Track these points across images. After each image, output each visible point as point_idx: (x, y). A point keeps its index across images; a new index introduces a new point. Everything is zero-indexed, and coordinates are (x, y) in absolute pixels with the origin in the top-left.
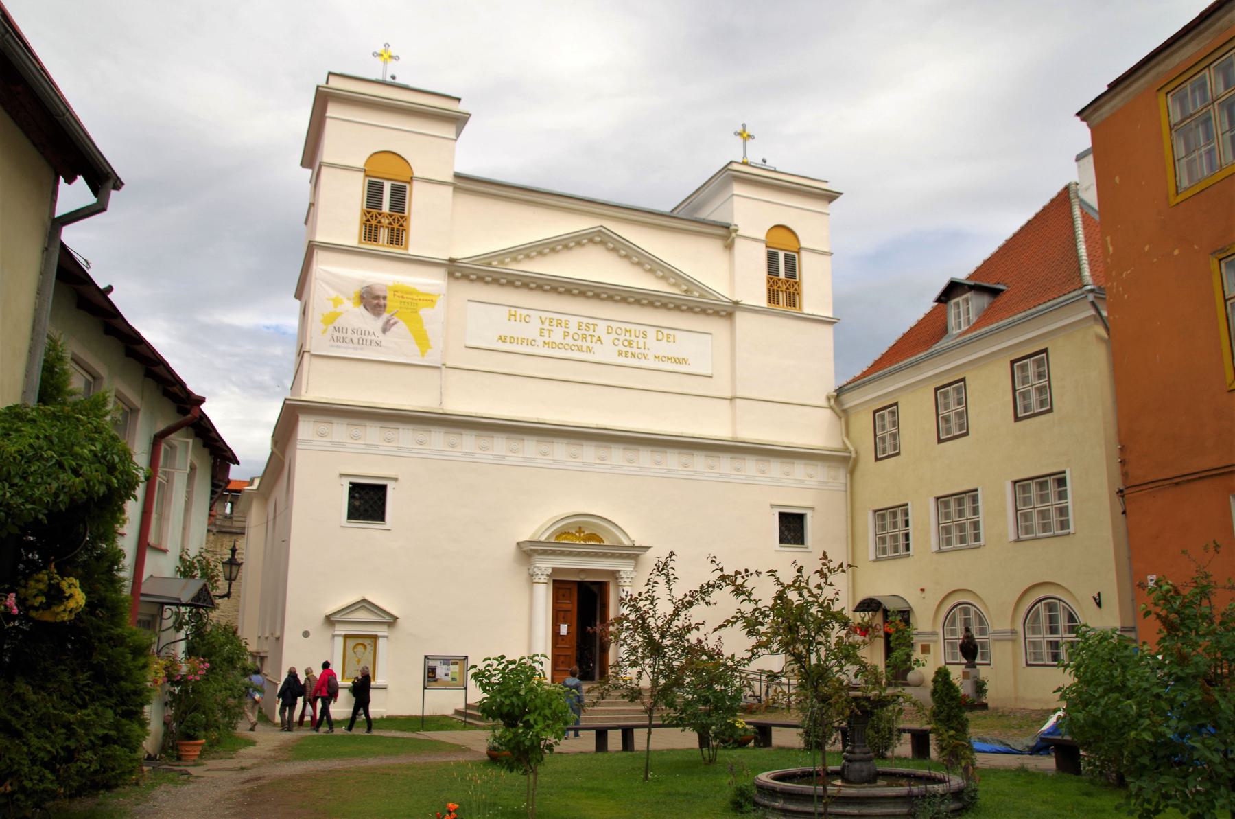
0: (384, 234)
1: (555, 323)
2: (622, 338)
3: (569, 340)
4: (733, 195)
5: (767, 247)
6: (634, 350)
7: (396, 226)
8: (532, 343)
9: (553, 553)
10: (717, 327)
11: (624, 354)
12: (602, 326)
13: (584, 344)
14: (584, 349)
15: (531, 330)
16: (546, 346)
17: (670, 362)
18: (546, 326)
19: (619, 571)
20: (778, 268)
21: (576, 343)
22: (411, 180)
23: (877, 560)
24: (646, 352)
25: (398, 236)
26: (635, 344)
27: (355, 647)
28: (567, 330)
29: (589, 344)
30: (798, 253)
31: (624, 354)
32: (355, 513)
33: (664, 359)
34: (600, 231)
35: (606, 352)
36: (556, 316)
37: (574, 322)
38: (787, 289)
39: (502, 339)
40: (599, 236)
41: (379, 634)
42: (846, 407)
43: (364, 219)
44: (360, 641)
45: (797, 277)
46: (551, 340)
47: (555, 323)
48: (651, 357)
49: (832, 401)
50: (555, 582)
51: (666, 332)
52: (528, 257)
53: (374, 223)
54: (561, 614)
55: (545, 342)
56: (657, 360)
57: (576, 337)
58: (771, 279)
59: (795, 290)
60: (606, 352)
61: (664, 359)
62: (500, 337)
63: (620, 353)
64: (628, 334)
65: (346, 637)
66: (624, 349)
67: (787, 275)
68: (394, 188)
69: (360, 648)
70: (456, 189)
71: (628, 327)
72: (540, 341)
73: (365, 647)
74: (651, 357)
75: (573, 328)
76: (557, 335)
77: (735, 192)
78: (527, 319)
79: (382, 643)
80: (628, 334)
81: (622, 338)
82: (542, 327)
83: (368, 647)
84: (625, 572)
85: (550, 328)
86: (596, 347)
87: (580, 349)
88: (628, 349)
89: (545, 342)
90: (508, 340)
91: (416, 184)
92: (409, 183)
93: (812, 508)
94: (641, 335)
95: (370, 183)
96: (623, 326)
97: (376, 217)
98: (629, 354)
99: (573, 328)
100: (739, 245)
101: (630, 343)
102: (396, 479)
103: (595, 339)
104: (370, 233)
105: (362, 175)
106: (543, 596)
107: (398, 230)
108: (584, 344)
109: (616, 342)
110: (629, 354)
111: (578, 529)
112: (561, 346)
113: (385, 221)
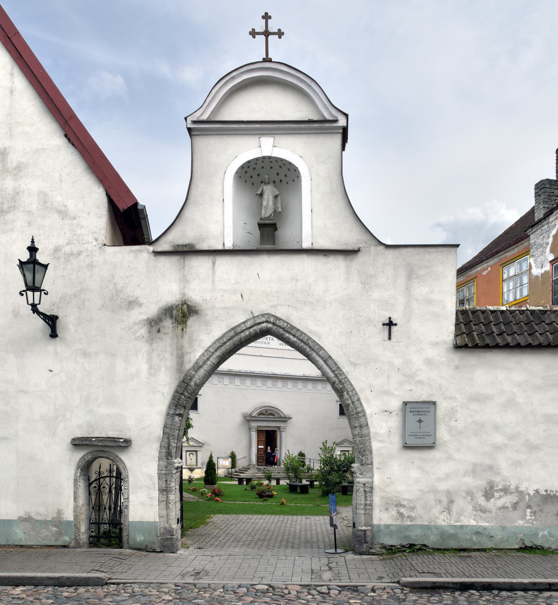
9: (258, 420)
14: (267, 343)
19: (280, 426)
27: (190, 454)
29: (268, 341)
44: (191, 452)
50: (258, 430)
54: (260, 442)
65: (187, 451)
69: (191, 455)
73: (193, 455)
79: (199, 453)
84: (283, 427)
87: (265, 343)
103: (271, 339)
106: (254, 435)
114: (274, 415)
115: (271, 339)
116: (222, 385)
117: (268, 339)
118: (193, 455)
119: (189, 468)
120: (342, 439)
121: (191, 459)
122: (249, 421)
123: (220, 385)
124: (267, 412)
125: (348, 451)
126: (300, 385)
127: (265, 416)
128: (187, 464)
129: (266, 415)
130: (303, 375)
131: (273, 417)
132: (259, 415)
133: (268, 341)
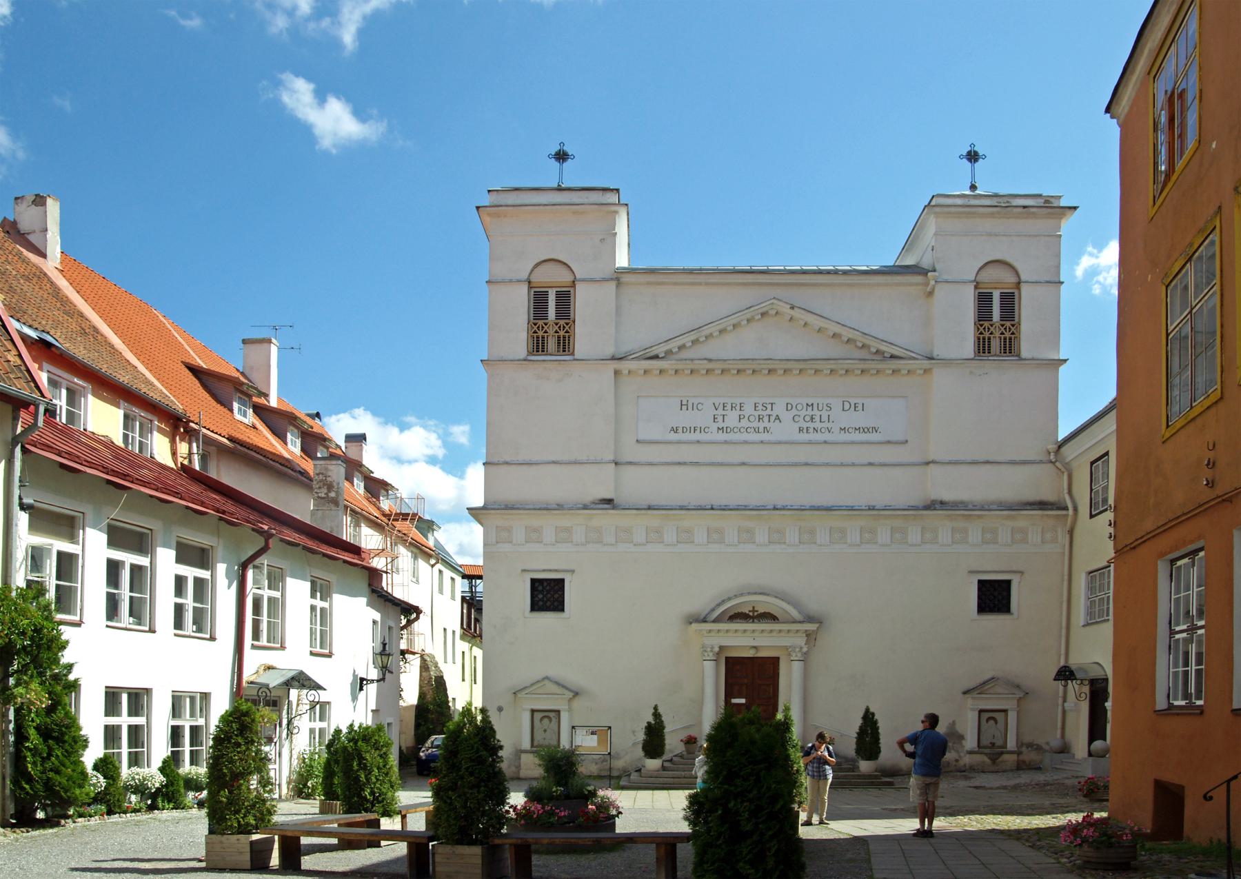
0: (551, 344)
1: (729, 407)
2: (803, 413)
3: (745, 423)
5: (976, 287)
6: (818, 425)
7: (562, 333)
11: (805, 431)
13: (761, 425)
15: (702, 417)
18: (720, 412)
22: (573, 284)
23: (1087, 625)
24: (829, 425)
25: (565, 345)
26: (817, 419)
27: (541, 719)
28: (742, 413)
29: (766, 424)
30: (1018, 288)
31: (805, 431)
32: (536, 606)
34: (773, 304)
35: (786, 429)
38: (1002, 334)
39: (674, 430)
42: (1067, 460)
43: (531, 333)
44: (546, 714)
45: (1016, 316)
47: (729, 407)
48: (836, 429)
49: (1052, 457)
58: (981, 325)
59: (1013, 334)
60: (786, 429)
64: (810, 408)
65: (533, 711)
66: (805, 425)
67: (1002, 318)
68: (558, 293)
69: (546, 721)
72: (714, 427)
73: (550, 720)
74: (836, 429)
75: (749, 409)
76: (732, 419)
80: (810, 408)
82: (716, 412)
83: (554, 719)
85: (724, 413)
86: (774, 426)
87: (757, 431)
88: (809, 424)
90: (680, 430)
93: (1022, 573)
94: (825, 408)
97: (543, 327)
98: (811, 430)
99: (749, 409)
100: (941, 292)
101: (812, 418)
102: (573, 571)
105: (525, 288)
107: (564, 337)
108: (761, 425)
111: (751, 609)
113: (551, 332)
115: (772, 419)
117: (766, 419)
118: (550, 720)
121: (545, 731)
124: (754, 611)
125: (1005, 711)
133: (766, 424)
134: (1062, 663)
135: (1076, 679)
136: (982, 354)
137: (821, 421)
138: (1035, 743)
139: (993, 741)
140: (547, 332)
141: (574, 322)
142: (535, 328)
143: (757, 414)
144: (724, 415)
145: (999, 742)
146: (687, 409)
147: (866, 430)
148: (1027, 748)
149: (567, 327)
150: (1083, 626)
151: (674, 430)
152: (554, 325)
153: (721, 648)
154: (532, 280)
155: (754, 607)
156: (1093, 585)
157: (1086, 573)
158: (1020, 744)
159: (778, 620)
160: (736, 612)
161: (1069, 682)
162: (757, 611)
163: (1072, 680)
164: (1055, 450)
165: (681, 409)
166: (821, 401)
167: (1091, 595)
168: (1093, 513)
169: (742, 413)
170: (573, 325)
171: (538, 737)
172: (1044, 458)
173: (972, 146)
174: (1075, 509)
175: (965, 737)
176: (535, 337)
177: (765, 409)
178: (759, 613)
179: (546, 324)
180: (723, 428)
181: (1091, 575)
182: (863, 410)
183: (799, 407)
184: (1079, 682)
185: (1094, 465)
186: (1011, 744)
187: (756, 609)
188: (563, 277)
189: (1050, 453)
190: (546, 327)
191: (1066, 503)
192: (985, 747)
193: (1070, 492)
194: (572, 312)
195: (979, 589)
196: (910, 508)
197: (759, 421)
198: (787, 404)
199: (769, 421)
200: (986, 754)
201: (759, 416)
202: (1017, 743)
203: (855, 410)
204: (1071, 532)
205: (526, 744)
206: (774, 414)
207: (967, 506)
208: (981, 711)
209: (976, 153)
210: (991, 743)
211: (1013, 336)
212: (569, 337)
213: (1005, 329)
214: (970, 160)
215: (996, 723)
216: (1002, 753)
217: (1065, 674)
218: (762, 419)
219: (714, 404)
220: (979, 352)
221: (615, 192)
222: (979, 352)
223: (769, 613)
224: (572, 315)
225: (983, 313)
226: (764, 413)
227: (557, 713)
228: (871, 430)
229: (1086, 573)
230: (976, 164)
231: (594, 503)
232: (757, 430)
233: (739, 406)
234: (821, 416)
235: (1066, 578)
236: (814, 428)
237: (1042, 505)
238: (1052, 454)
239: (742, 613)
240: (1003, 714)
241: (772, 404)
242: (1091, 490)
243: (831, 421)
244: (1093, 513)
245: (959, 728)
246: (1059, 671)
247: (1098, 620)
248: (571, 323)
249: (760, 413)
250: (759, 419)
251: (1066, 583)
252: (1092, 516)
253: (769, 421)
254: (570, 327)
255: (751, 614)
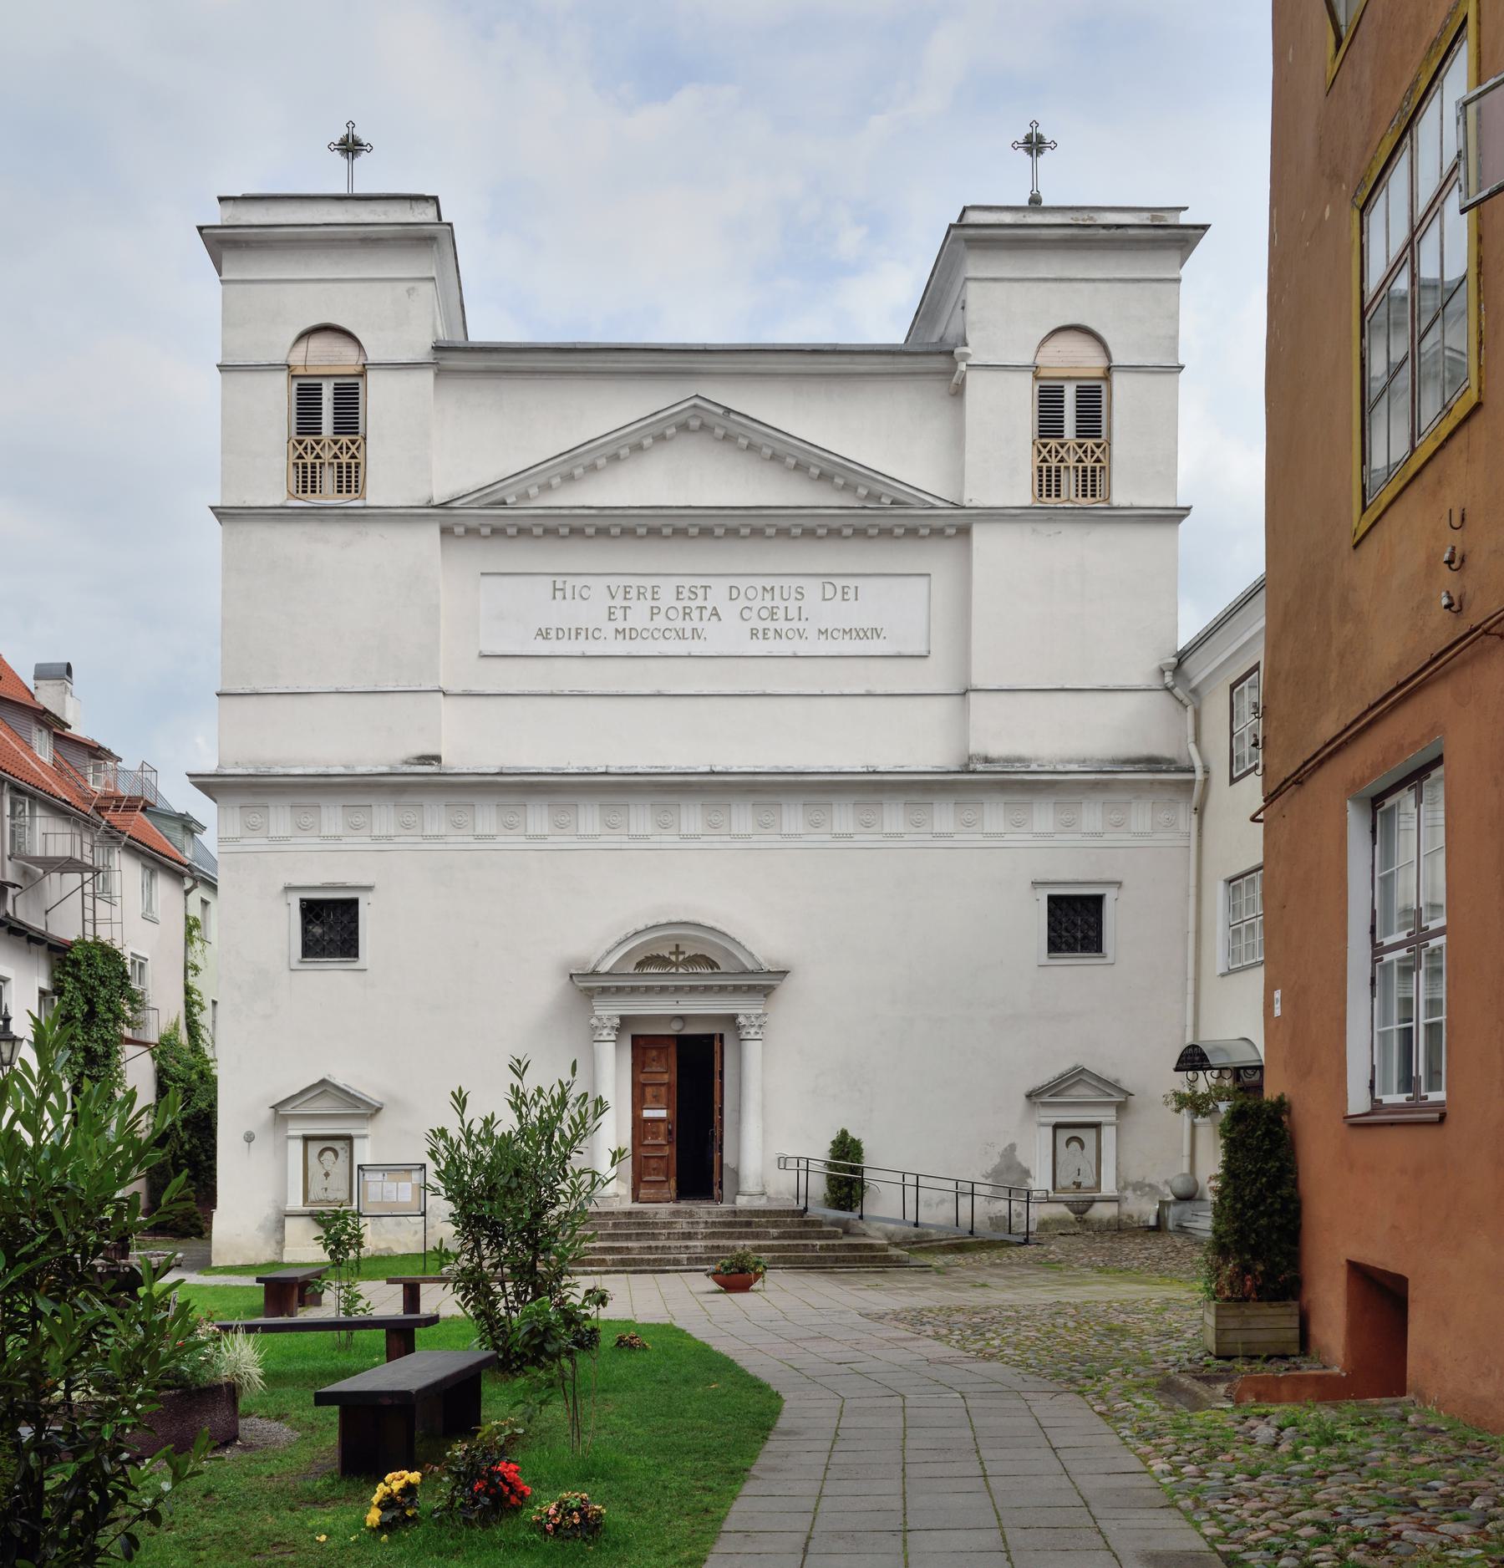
0: (328, 478)
1: (633, 593)
2: (756, 604)
3: (660, 622)
4: (967, 279)
6: (782, 625)
7: (345, 459)
8: (593, 634)
10: (936, 559)
11: (760, 635)
12: (720, 588)
13: (688, 626)
14: (688, 634)
16: (620, 637)
17: (847, 637)
18: (619, 601)
20: (1060, 421)
21: (670, 625)
22: (362, 375)
24: (801, 625)
25: (350, 477)
26: (781, 614)
28: (655, 603)
29: (696, 624)
31: (760, 635)
32: (312, 948)
33: (835, 634)
36: (634, 582)
37: (667, 588)
39: (543, 634)
40: (695, 416)
41: (353, 1132)
44: (328, 1144)
46: (627, 625)
47: (633, 593)
48: (812, 633)
50: (635, 1038)
51: (839, 583)
52: (569, 478)
53: (309, 459)
54: (649, 1091)
55: (617, 631)
56: (823, 637)
57: (672, 614)
61: (835, 634)
62: (540, 633)
63: (754, 633)
64: (768, 596)
65: (307, 1139)
66: (761, 625)
68: (338, 389)
69: (329, 1155)
70: (441, 373)
71: (768, 582)
72: (609, 629)
74: (812, 633)
75: (667, 597)
77: (970, 274)
78: (585, 593)
80: (768, 596)
81: (756, 604)
82: (612, 604)
83: (341, 1153)
85: (626, 604)
86: (709, 627)
89: (617, 631)
90: (553, 634)
91: (372, 376)
92: (362, 376)
93: (1118, 884)
94: (794, 594)
95: (301, 389)
96: (759, 583)
98: (771, 634)
99: (667, 597)
103: (706, 614)
104: (307, 479)
107: (349, 466)
108: (688, 626)
109: (746, 614)
110: (771, 634)
111: (674, 950)
112: (645, 634)
113: (327, 456)
114: (713, 964)
115: (706, 614)
116: (466, 839)
117: (695, 614)
119: (311, 1215)
120: (1064, 1066)
121: (327, 1175)
122: (589, 994)
123: (460, 839)
124: (677, 952)
126: (843, 817)
127: (673, 970)
128: (312, 1197)
129: (676, 965)
130: (865, 770)
131: (710, 971)
132: (640, 965)
134: (1189, 1041)
135: (1211, 1068)
136: (1044, 498)
137: (786, 619)
138: (1147, 1181)
139: (1079, 1180)
140: (320, 458)
141: (365, 439)
142: (300, 448)
143: (680, 605)
144: (625, 608)
145: (1088, 1181)
146: (564, 598)
147: (862, 634)
148: (1134, 1190)
149: (353, 448)
150: (1223, 975)
151: (543, 634)
152: (332, 444)
153: (622, 1018)
154: (291, 363)
155: (677, 946)
156: (1238, 901)
157: (1225, 881)
158: (1123, 1185)
159: (718, 968)
160: (649, 955)
161: (1201, 1073)
162: (683, 953)
163: (1204, 1069)
164: (1173, 667)
165: (554, 598)
166: (785, 582)
167: (1233, 920)
168: (1236, 775)
169: (655, 603)
170: (362, 444)
171: (316, 1192)
172: (1156, 684)
173: (1034, 125)
174: (1206, 771)
175: (1032, 1173)
176: (300, 466)
177: (693, 596)
178: (686, 956)
179: (318, 444)
180: (624, 630)
181: (1232, 884)
182: (856, 599)
183: (751, 593)
184: (1216, 1073)
185: (1236, 690)
186: (1108, 1187)
187: (681, 949)
188: (342, 357)
189: (1163, 672)
190: (318, 448)
191: (1191, 759)
192: (1065, 1189)
193: (1197, 741)
194: (361, 421)
195: (1051, 913)
196: (935, 770)
197: (684, 619)
198: (731, 587)
199: (701, 619)
200: (1067, 1203)
201: (684, 608)
202: (1117, 1183)
203: (844, 599)
204: (1200, 811)
205: (296, 1202)
206: (709, 605)
207: (1029, 766)
208: (1057, 1127)
209: (1040, 139)
210: (1074, 1183)
211: (1098, 465)
212: (356, 467)
213: (1085, 452)
214: (1029, 151)
215: (1082, 1147)
216: (1093, 1201)
217: (1193, 1059)
218: (689, 614)
219: (609, 587)
220: (1041, 496)
221: (431, 202)
222: (1077, 496)
223: (703, 956)
224: (361, 430)
225: (1049, 424)
226: (693, 604)
227: (348, 1141)
228: (869, 634)
229: (1225, 881)
230: (1041, 158)
231: (406, 763)
232: (681, 636)
233: (650, 591)
234: (786, 608)
235: (1193, 891)
236: (776, 631)
237: (1152, 763)
238: (1167, 674)
239: (658, 957)
240: (1092, 1133)
241: (705, 587)
242: (1232, 734)
243: (803, 618)
244: (1236, 775)
245: (1021, 1157)
246: (1182, 1056)
247: (1245, 963)
248: (360, 440)
249: (686, 603)
250: (685, 614)
251: (1192, 901)
252: (1233, 781)
253: (701, 619)
254: (357, 449)
255: (673, 958)
